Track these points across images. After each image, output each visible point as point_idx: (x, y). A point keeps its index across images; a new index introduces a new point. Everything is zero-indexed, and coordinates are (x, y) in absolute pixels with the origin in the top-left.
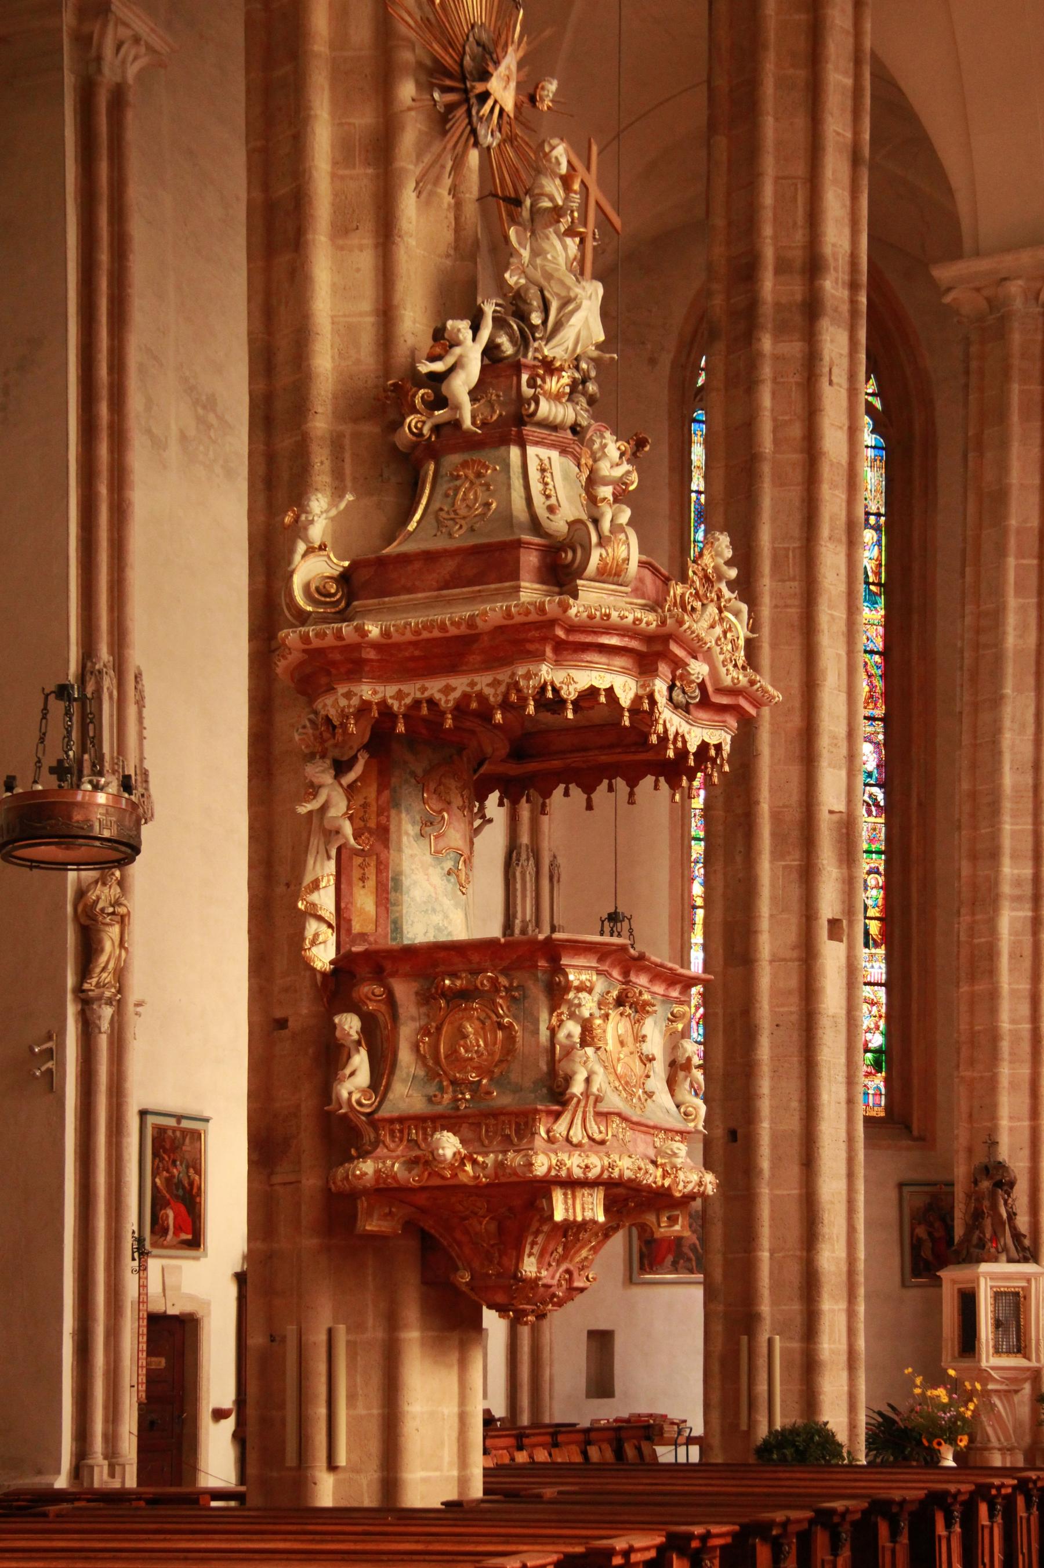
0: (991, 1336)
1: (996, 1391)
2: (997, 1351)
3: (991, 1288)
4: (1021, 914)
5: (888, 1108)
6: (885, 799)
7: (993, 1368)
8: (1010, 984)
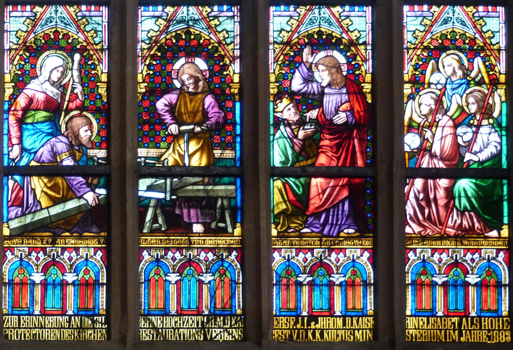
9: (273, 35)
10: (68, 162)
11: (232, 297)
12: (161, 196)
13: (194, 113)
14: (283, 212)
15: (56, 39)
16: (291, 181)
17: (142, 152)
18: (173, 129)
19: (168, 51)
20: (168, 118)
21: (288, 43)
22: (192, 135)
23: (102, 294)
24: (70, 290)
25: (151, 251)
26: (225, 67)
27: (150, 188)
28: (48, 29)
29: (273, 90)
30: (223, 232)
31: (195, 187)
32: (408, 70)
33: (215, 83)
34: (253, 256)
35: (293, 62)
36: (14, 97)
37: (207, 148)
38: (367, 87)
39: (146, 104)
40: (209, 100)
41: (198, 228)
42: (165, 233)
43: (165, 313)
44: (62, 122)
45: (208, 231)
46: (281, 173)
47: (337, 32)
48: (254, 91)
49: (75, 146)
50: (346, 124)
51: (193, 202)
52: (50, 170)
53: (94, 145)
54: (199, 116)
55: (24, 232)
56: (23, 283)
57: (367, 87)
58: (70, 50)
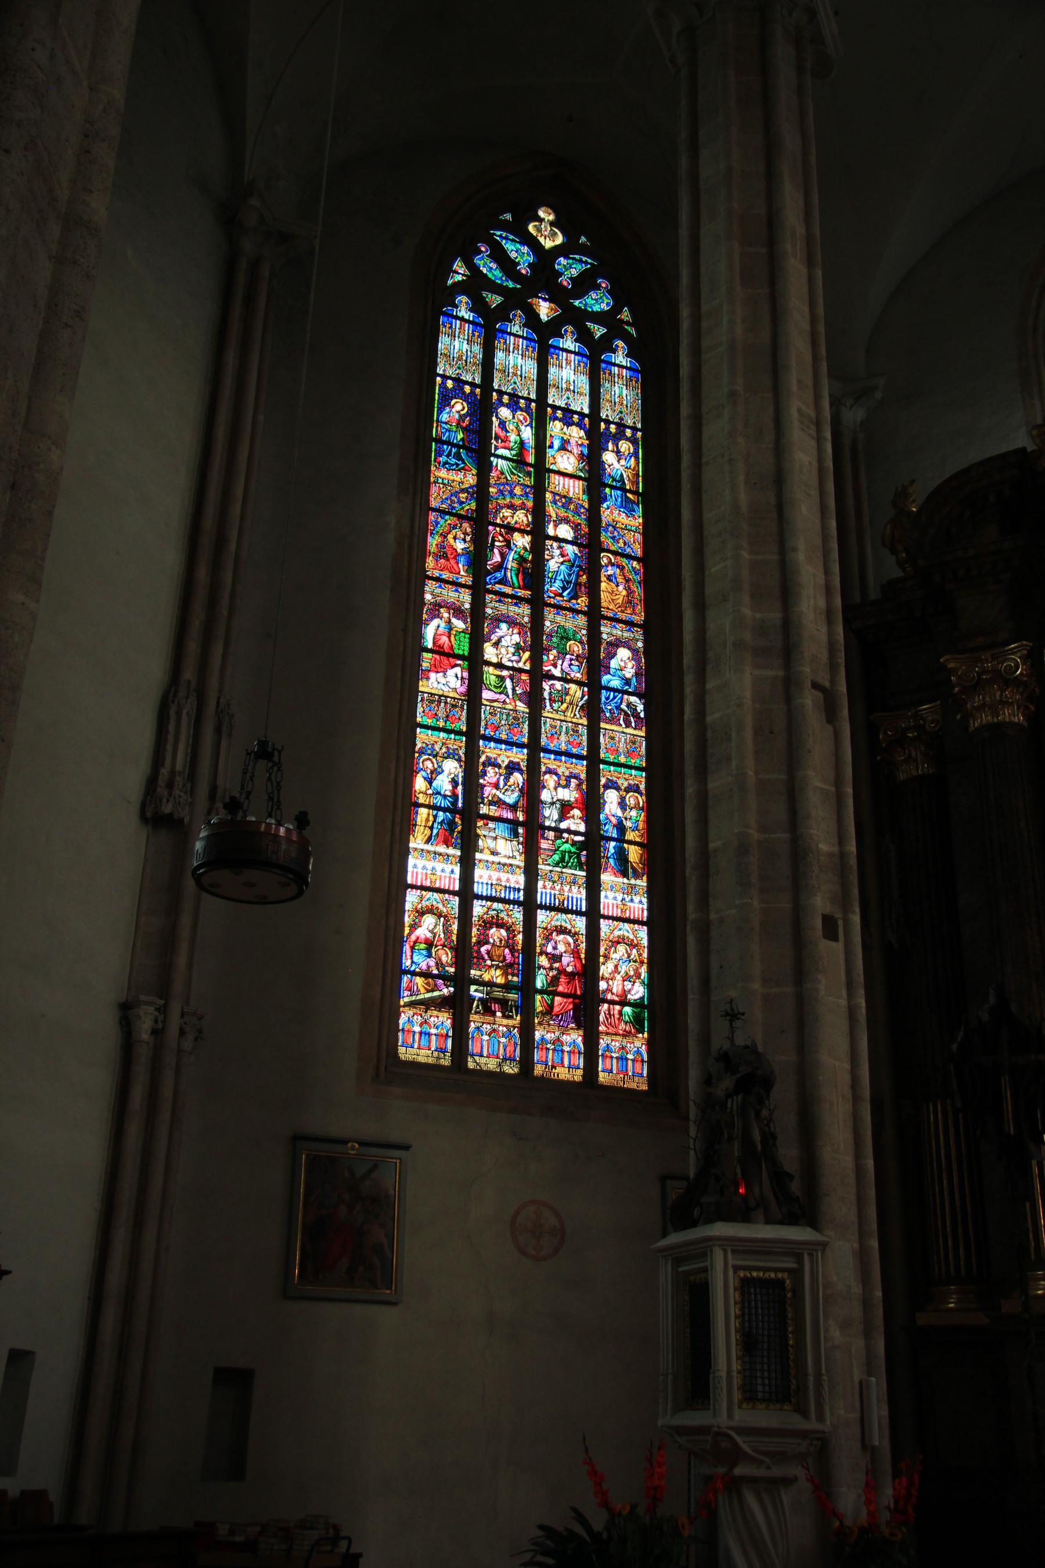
0: (736, 1366)
1: (754, 1481)
2: (750, 1396)
3: (736, 1269)
4: (770, 673)
5: (652, 1078)
6: (645, 710)
7: (741, 1431)
8: (756, 773)
9: (539, 923)
10: (435, 972)
12: (481, 995)
14: (541, 1012)
15: (432, 909)
17: (473, 972)
18: (489, 962)
19: (488, 924)
20: (486, 957)
21: (546, 928)
22: (498, 967)
23: (450, 1042)
24: (433, 1038)
26: (515, 936)
27: (476, 991)
29: (538, 950)
30: (511, 1017)
31: (498, 994)
33: (510, 944)
34: (526, 1031)
35: (548, 938)
36: (409, 934)
37: (505, 974)
40: (507, 951)
41: (499, 1014)
42: (483, 1014)
43: (481, 1056)
44: (433, 951)
45: (504, 1016)
46: (541, 992)
47: (569, 927)
48: (529, 949)
49: (439, 964)
51: (497, 1000)
52: (426, 975)
54: (501, 958)
55: (411, 1004)
56: (409, 1031)
57: (583, 956)
58: (439, 915)
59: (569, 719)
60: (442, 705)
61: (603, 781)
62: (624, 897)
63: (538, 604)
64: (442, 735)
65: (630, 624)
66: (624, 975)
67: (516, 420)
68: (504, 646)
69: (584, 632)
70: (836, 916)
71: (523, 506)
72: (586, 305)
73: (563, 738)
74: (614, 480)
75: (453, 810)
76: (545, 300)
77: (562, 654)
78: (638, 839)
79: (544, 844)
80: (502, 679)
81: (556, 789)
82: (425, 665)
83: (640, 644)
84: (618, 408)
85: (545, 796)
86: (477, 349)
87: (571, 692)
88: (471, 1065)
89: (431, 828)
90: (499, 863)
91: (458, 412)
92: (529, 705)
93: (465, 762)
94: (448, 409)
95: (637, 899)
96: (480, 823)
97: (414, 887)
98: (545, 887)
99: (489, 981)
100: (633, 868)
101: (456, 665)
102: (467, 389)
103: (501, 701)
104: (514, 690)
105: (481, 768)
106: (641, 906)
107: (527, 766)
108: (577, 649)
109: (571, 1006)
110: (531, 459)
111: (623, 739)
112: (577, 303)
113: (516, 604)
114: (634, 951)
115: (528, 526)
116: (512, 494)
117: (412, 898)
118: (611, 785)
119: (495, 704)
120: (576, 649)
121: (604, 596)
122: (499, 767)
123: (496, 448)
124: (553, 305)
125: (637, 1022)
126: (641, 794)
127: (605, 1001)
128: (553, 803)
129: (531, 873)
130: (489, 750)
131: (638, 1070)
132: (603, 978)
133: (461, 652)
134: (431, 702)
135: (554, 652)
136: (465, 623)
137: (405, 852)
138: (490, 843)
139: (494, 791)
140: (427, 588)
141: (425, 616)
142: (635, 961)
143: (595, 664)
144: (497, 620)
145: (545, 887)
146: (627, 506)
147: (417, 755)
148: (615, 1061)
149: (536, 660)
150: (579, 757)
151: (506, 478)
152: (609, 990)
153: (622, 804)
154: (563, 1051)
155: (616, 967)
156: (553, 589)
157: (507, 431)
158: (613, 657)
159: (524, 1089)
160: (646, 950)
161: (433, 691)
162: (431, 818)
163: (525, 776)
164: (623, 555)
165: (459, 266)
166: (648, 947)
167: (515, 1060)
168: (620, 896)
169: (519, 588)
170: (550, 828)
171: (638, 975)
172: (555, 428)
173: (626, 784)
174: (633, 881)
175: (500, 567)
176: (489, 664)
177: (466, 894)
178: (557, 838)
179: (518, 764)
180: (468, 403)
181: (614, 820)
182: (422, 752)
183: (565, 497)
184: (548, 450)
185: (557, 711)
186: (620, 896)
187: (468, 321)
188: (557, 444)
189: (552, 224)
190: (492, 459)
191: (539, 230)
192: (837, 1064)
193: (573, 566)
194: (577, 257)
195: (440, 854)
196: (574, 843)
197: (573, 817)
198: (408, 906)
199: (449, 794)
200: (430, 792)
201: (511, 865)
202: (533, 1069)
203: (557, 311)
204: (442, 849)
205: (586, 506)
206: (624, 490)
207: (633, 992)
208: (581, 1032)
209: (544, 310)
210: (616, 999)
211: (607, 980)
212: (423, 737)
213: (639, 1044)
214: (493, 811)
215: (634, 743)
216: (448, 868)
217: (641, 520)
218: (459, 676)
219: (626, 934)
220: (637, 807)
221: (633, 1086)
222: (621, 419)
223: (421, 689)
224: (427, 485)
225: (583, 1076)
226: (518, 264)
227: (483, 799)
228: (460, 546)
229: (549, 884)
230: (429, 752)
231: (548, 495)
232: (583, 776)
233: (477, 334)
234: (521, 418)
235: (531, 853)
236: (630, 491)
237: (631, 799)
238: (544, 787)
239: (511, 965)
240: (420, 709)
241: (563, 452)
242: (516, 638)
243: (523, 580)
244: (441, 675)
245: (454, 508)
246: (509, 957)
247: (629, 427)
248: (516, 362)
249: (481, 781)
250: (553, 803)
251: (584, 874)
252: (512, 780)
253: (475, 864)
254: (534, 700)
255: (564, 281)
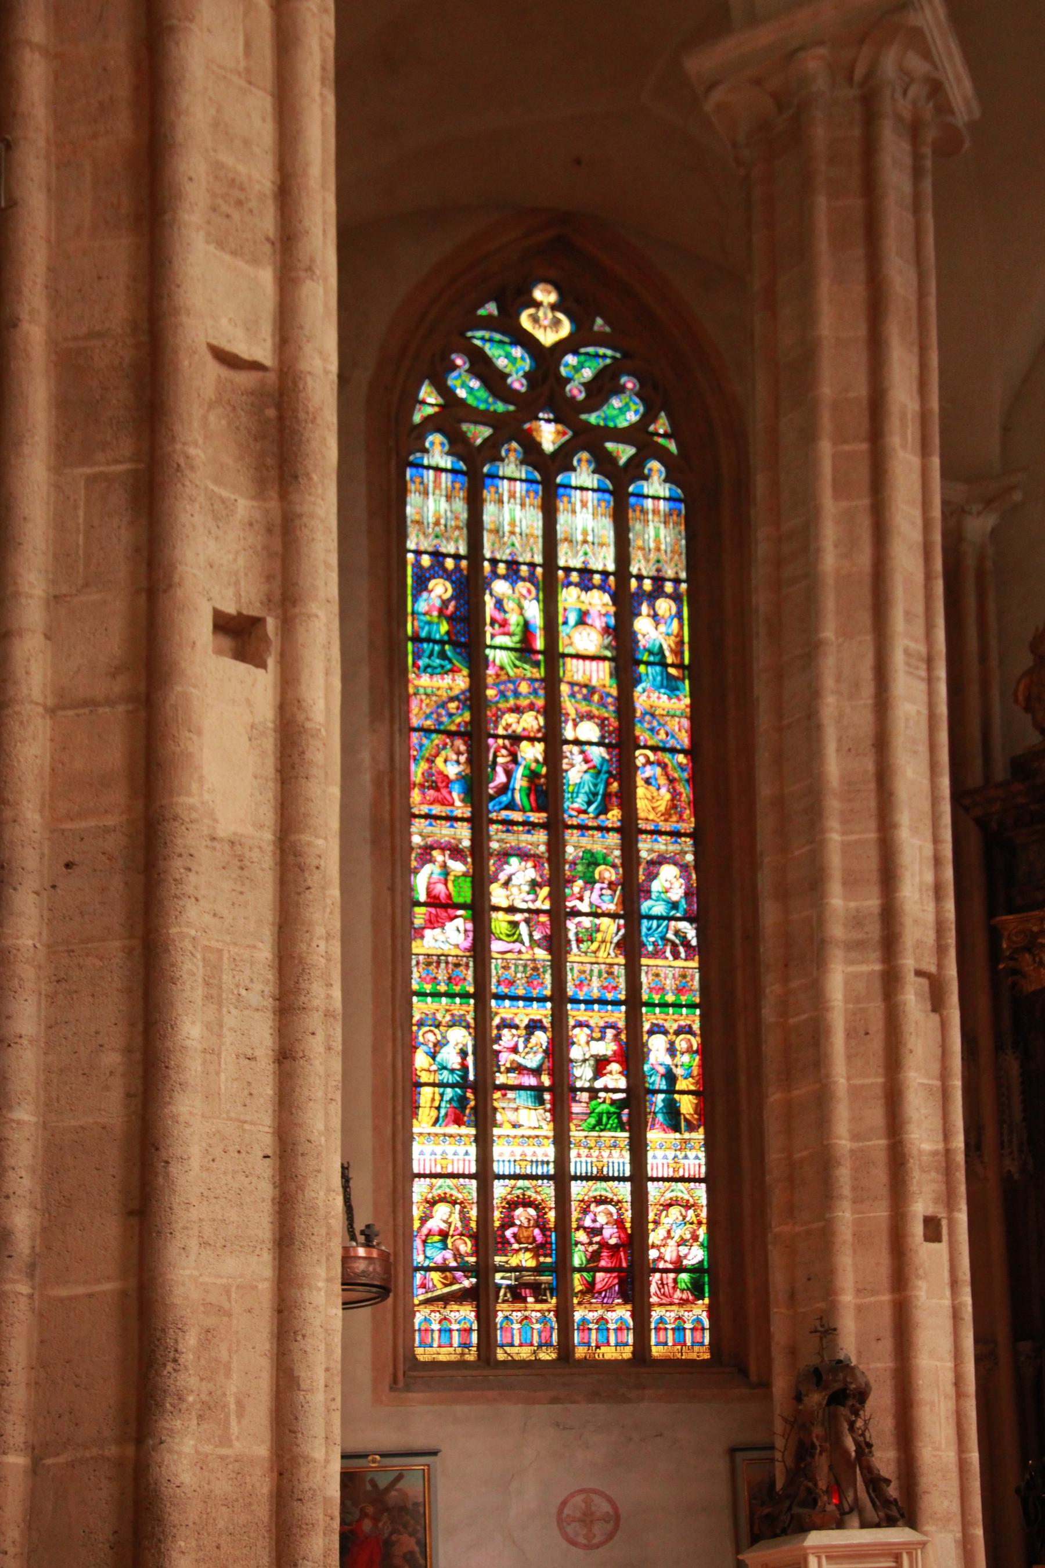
6: (698, 936)
9: (574, 1196)
10: (453, 1264)
11: (551, 1336)
12: (508, 1282)
13: (528, 1238)
14: (581, 1291)
16: (585, 1274)
17: (497, 1259)
18: (516, 1246)
19: (512, 1205)
20: (512, 1240)
21: (582, 1201)
22: (527, 1250)
24: (455, 1334)
25: (502, 1312)
26: (546, 1213)
27: (503, 1278)
28: (440, 1192)
29: (574, 1225)
30: (545, 1301)
31: (529, 1278)
32: (651, 1216)
33: (540, 1223)
35: (585, 1211)
36: (420, 1228)
37: (536, 1256)
38: (628, 1225)
39: (499, 1233)
40: (537, 1231)
42: (512, 1302)
43: (512, 1345)
44: (449, 1241)
45: (537, 1301)
46: (580, 1270)
47: (610, 1195)
49: (457, 1255)
50: (616, 1244)
51: (527, 1285)
52: (443, 1268)
53: (468, 1255)
54: (531, 1240)
55: (427, 1302)
56: (426, 1330)
57: (628, 1225)
58: (454, 1203)
59: (601, 960)
60: (443, 965)
61: (647, 1026)
62: (677, 1155)
63: (555, 828)
64: (444, 1000)
65: (676, 834)
66: (678, 1237)
67: (517, 595)
68: (516, 885)
69: (617, 853)
70: (940, 1216)
71: (531, 707)
72: (605, 419)
73: (595, 983)
74: (651, 653)
75: (463, 1084)
76: (548, 421)
77: (590, 882)
78: (692, 1088)
79: (576, 1108)
80: (515, 925)
81: (588, 1043)
82: (418, 922)
83: (690, 858)
84: (653, 556)
85: (575, 1053)
86: (460, 507)
87: (603, 928)
88: (501, 1356)
89: (438, 1108)
90: (523, 1136)
91: (440, 597)
92: (550, 950)
93: (475, 1028)
94: (425, 595)
95: (692, 1154)
96: (497, 1095)
97: (420, 1176)
98: (579, 1155)
99: (518, 1266)
100: (686, 1120)
101: (457, 917)
102: (450, 563)
103: (514, 950)
104: (531, 935)
105: (495, 1032)
106: (697, 1162)
107: (552, 1023)
108: (610, 874)
109: (616, 1281)
110: (539, 644)
111: (670, 973)
112: (593, 419)
113: (529, 832)
114: (691, 1213)
115: (539, 731)
116: (517, 694)
117: (420, 1189)
118: (657, 1029)
119: (508, 956)
120: (607, 875)
121: (642, 805)
122: (517, 1027)
123: (493, 636)
124: (560, 427)
125: (697, 1290)
126: (693, 1034)
127: (657, 1270)
128: (585, 1061)
129: (562, 1141)
130: (503, 1010)
131: (698, 1339)
132: (653, 1247)
133: (461, 900)
134: (429, 964)
135: (580, 883)
136: (465, 863)
137: (410, 1138)
138: (511, 1116)
139: (513, 1056)
140: (413, 829)
141: (414, 864)
142: (692, 1223)
143: (632, 890)
144: (504, 855)
145: (579, 1155)
146: (670, 685)
147: (415, 1028)
148: (670, 1333)
149: (557, 897)
150: (616, 1003)
151: (507, 674)
152: (660, 1258)
153: (672, 1050)
154: (608, 1329)
155: (669, 1232)
156: (575, 806)
157: (505, 612)
158: (655, 878)
159: (566, 1373)
160: (705, 1210)
161: (430, 952)
162: (437, 1097)
163: (549, 1034)
164: (664, 750)
165: (428, 394)
166: (708, 1205)
167: (552, 1346)
168: (671, 1154)
169: (532, 810)
170: (582, 1090)
171: (695, 1238)
172: (569, 598)
173: (675, 1026)
174: (687, 1135)
175: (504, 789)
176: (497, 909)
177: (485, 1175)
178: (591, 1098)
179: (540, 1021)
180: (452, 582)
181: (662, 1070)
182: (421, 1024)
183: (586, 686)
184: (561, 628)
185: (586, 953)
186: (671, 1154)
187: (446, 470)
188: (572, 618)
189: (554, 307)
190: (488, 651)
191: (535, 320)
192: (939, 1364)
193: (599, 772)
194: (591, 350)
195: (451, 1136)
196: (613, 1102)
197: (611, 1073)
198: (416, 1198)
199: (458, 1067)
200: (434, 1067)
201: (537, 1137)
202: (574, 1353)
203: (564, 434)
204: (453, 1129)
205: (615, 693)
206: (664, 664)
207: (689, 1257)
208: (629, 1307)
209: (549, 435)
210: (670, 1266)
211: (658, 1247)
212: (420, 1008)
213: (699, 1311)
214: (512, 1079)
215: (684, 976)
216: (461, 1149)
217: (688, 701)
218: (462, 929)
219: (680, 1195)
220: (689, 1050)
221: (693, 1356)
222: (658, 570)
223: (415, 951)
224: (406, 699)
225: (633, 1353)
226: (508, 375)
227: (499, 1067)
228: (452, 770)
229: (584, 1152)
230: (430, 1022)
231: (564, 689)
232: (621, 1024)
233: (457, 486)
234: (524, 592)
235: (561, 1119)
236: (673, 665)
237: (681, 1043)
238: (573, 1043)
239: (542, 1246)
240: (415, 975)
241: (581, 628)
242: (531, 874)
243: (536, 801)
244: (438, 931)
245: (441, 723)
246: (539, 1238)
247: (669, 580)
248: (513, 515)
249: (496, 1047)
250: (585, 1061)
251: (627, 1134)
252: (533, 1040)
253: (493, 1141)
254: (556, 944)
255: (575, 390)
